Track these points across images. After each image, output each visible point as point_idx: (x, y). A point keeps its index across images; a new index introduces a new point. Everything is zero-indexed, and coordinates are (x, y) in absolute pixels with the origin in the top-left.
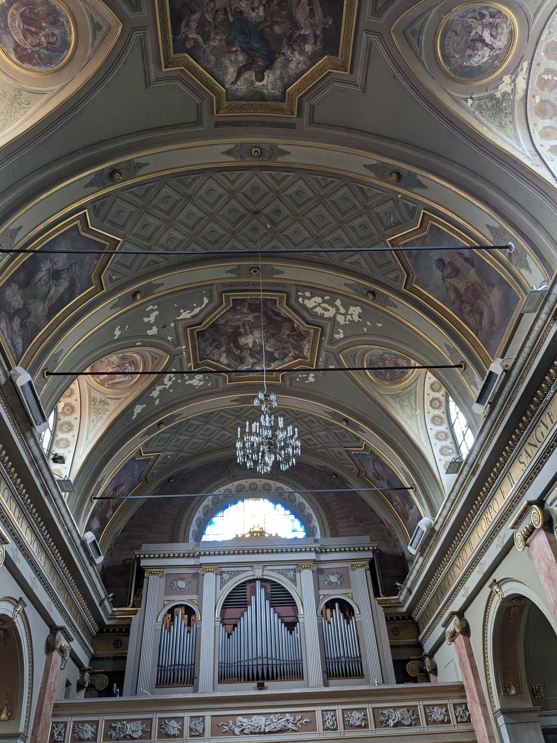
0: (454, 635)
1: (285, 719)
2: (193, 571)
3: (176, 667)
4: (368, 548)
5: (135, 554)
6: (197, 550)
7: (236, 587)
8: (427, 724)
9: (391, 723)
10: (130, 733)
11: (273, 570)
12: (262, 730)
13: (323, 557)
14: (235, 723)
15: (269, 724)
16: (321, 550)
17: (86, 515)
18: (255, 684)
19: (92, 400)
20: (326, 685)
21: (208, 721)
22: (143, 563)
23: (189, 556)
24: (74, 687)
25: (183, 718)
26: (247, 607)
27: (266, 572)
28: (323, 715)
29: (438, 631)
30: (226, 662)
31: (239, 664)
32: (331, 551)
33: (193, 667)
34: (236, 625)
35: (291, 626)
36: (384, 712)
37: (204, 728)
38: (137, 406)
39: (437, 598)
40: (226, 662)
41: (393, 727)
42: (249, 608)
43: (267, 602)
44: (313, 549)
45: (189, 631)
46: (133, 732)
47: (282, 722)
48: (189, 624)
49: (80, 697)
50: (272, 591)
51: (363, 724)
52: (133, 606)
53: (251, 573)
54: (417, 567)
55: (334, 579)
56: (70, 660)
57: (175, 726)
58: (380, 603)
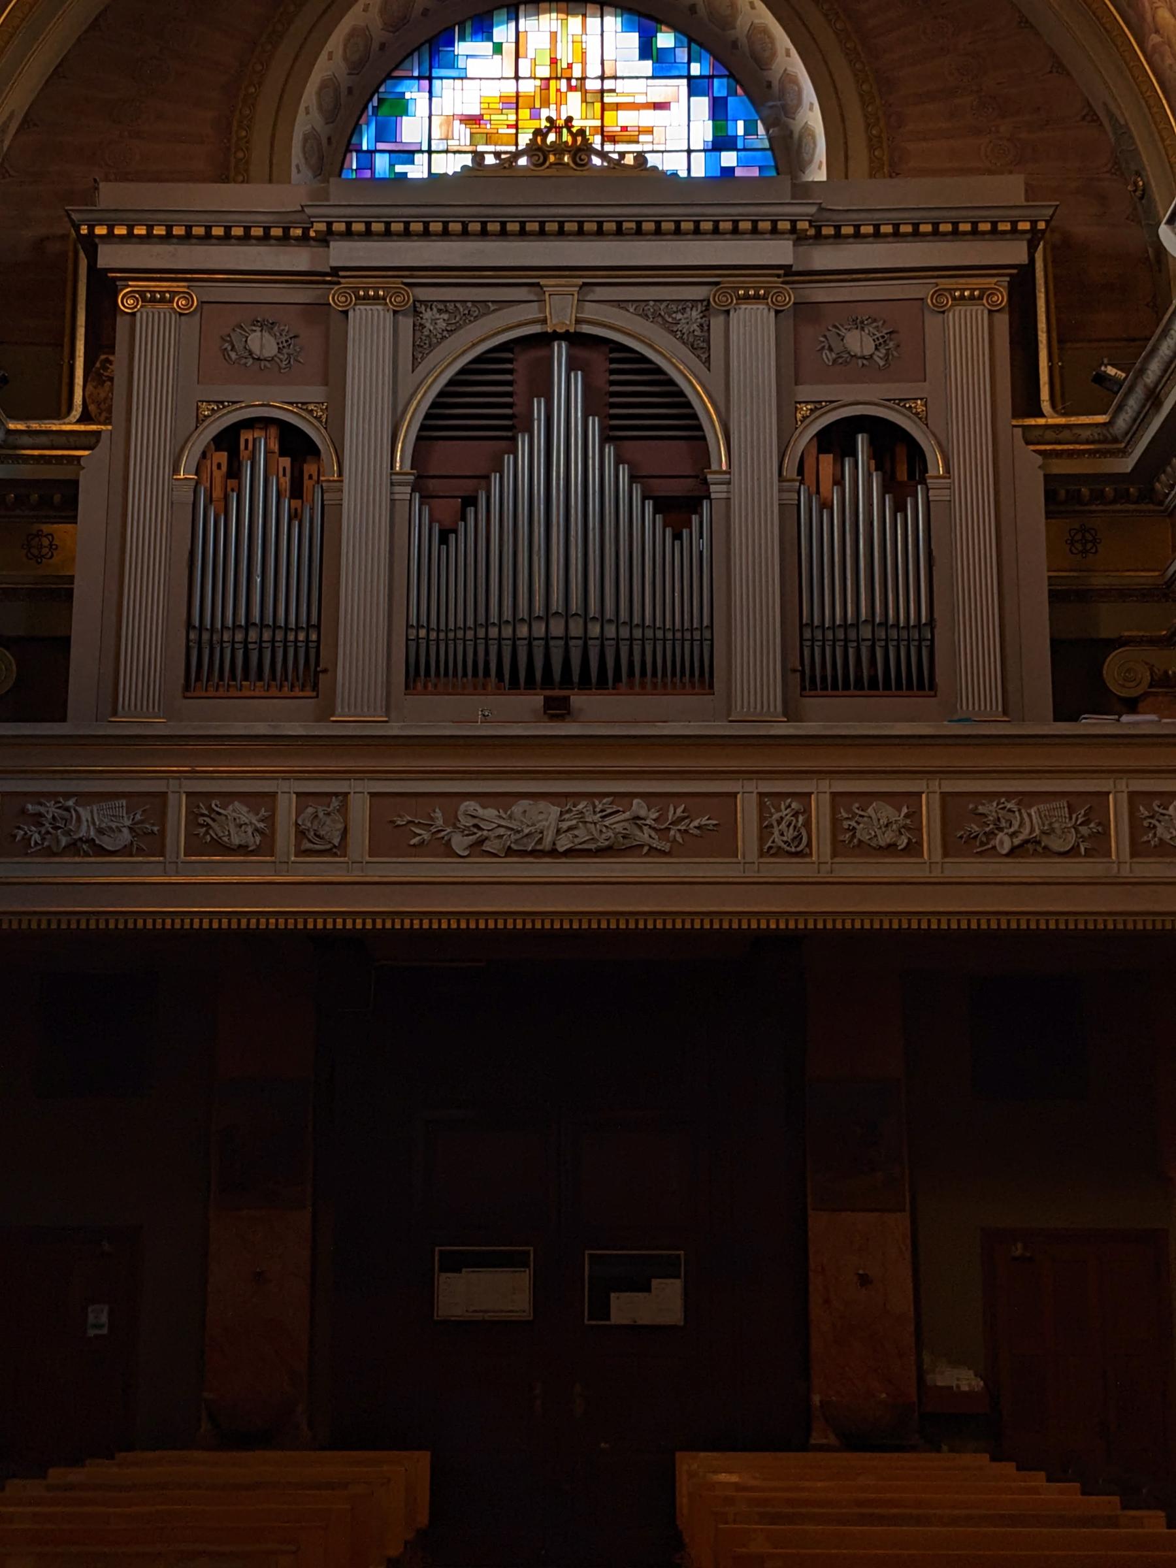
1: (627, 815)
3: (253, 635)
4: (1014, 224)
5: (72, 221)
7: (471, 362)
8: (1133, 854)
9: (1004, 843)
10: (92, 833)
11: (619, 303)
12: (547, 844)
13: (824, 258)
14: (453, 820)
15: (570, 829)
16: (818, 229)
18: (536, 700)
20: (791, 713)
21: (360, 811)
22: (108, 257)
23: (285, 239)
25: (273, 795)
26: (514, 439)
27: (591, 311)
28: (762, 807)
30: (433, 625)
31: (481, 633)
32: (857, 235)
33: (314, 637)
34: (470, 501)
36: (981, 809)
37: (345, 832)
40: (433, 625)
41: (1007, 855)
42: (522, 443)
43: (594, 423)
44: (784, 225)
45: (294, 515)
46: (100, 831)
47: (618, 822)
48: (297, 491)
50: (612, 383)
51: (903, 842)
52: (85, 418)
53: (531, 311)
55: (859, 342)
57: (244, 819)
58: (1030, 436)
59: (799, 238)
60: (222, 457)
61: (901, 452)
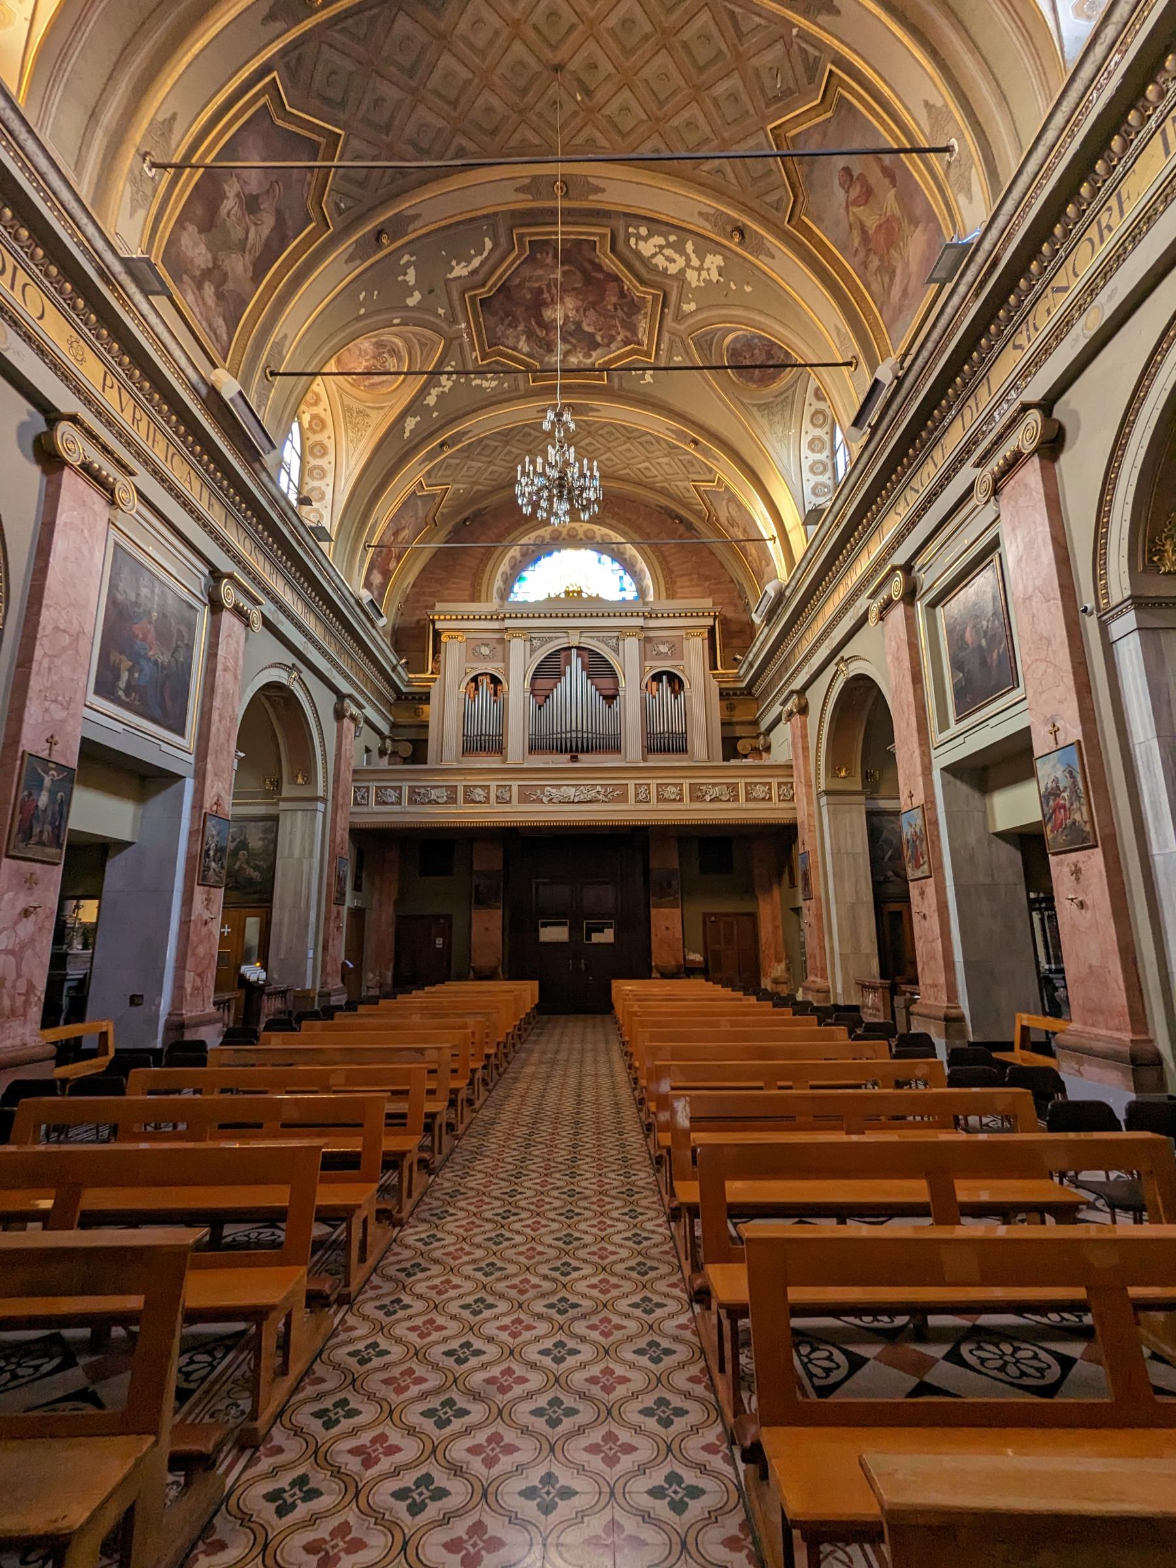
0: (791, 714)
2: (497, 636)
6: (507, 609)
13: (653, 623)
17: (361, 567)
18: (568, 756)
19: (347, 410)
20: (644, 760)
22: (438, 625)
24: (375, 752)
27: (583, 640)
29: (777, 709)
34: (548, 697)
35: (610, 698)
38: (409, 419)
39: (780, 673)
42: (563, 679)
43: (584, 673)
45: (495, 701)
48: (496, 694)
49: (384, 763)
52: (432, 673)
53: (565, 640)
54: (762, 638)
56: (366, 726)
59: (645, 617)
60: (473, 684)
61: (677, 681)
